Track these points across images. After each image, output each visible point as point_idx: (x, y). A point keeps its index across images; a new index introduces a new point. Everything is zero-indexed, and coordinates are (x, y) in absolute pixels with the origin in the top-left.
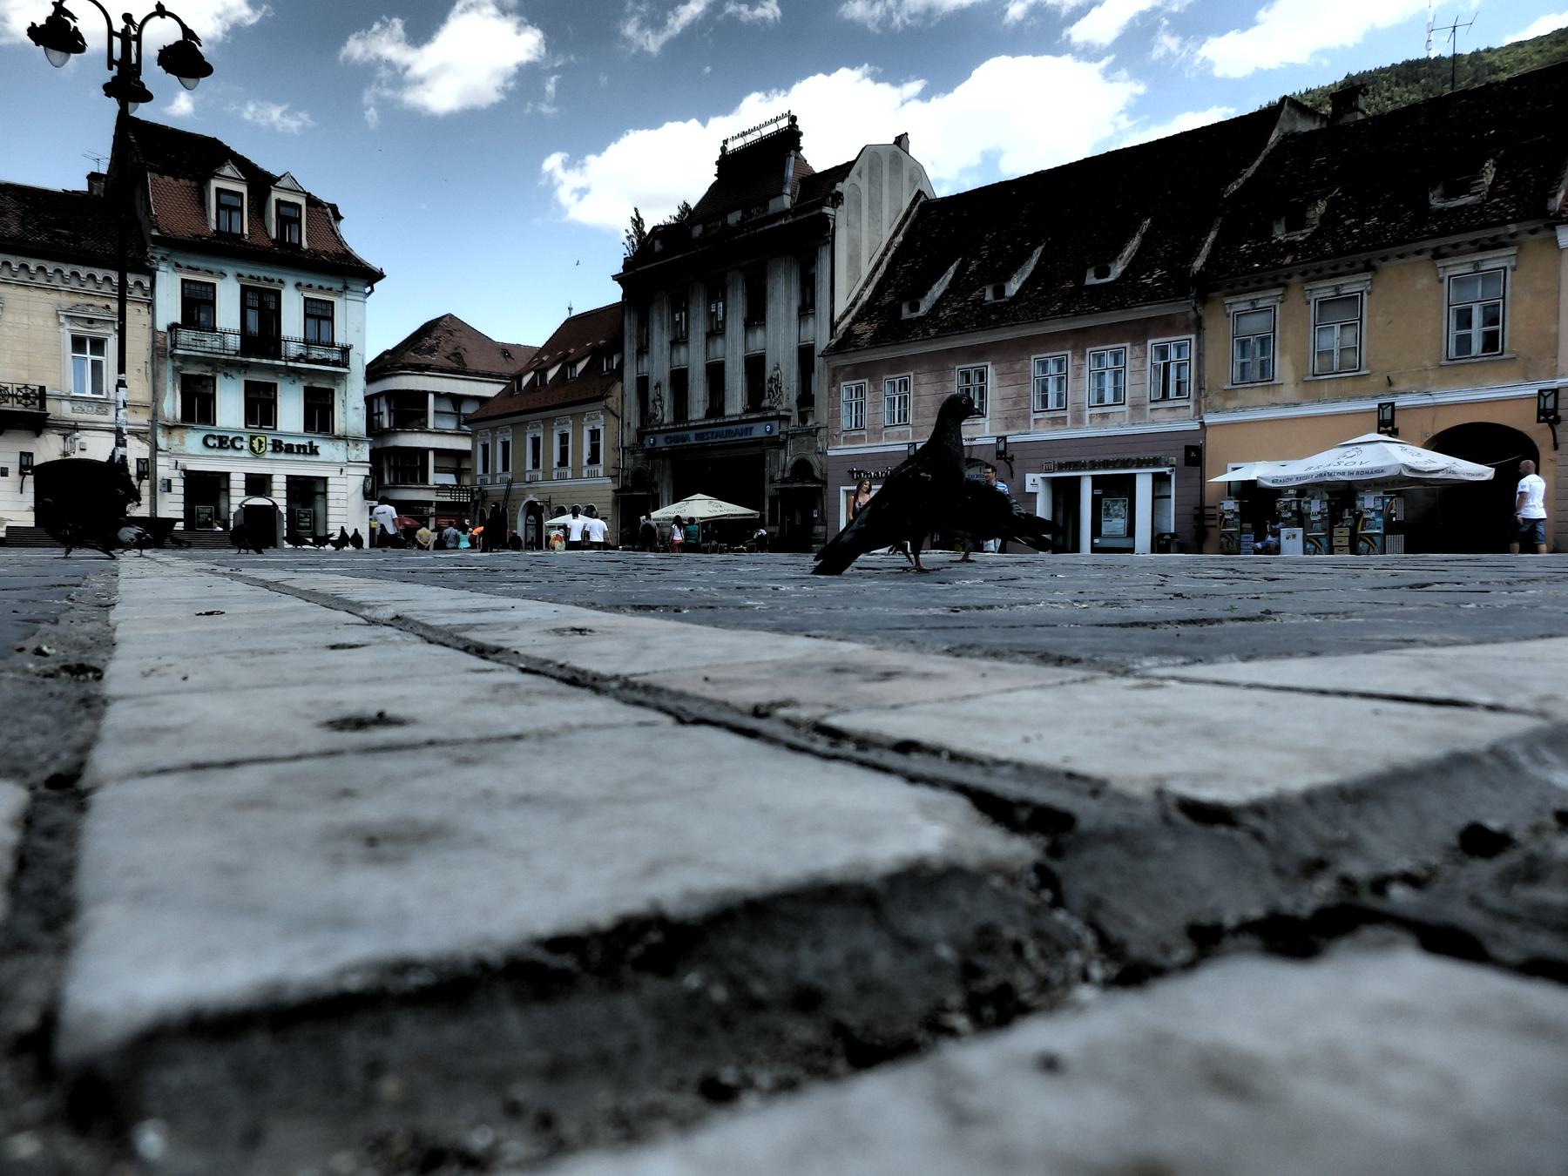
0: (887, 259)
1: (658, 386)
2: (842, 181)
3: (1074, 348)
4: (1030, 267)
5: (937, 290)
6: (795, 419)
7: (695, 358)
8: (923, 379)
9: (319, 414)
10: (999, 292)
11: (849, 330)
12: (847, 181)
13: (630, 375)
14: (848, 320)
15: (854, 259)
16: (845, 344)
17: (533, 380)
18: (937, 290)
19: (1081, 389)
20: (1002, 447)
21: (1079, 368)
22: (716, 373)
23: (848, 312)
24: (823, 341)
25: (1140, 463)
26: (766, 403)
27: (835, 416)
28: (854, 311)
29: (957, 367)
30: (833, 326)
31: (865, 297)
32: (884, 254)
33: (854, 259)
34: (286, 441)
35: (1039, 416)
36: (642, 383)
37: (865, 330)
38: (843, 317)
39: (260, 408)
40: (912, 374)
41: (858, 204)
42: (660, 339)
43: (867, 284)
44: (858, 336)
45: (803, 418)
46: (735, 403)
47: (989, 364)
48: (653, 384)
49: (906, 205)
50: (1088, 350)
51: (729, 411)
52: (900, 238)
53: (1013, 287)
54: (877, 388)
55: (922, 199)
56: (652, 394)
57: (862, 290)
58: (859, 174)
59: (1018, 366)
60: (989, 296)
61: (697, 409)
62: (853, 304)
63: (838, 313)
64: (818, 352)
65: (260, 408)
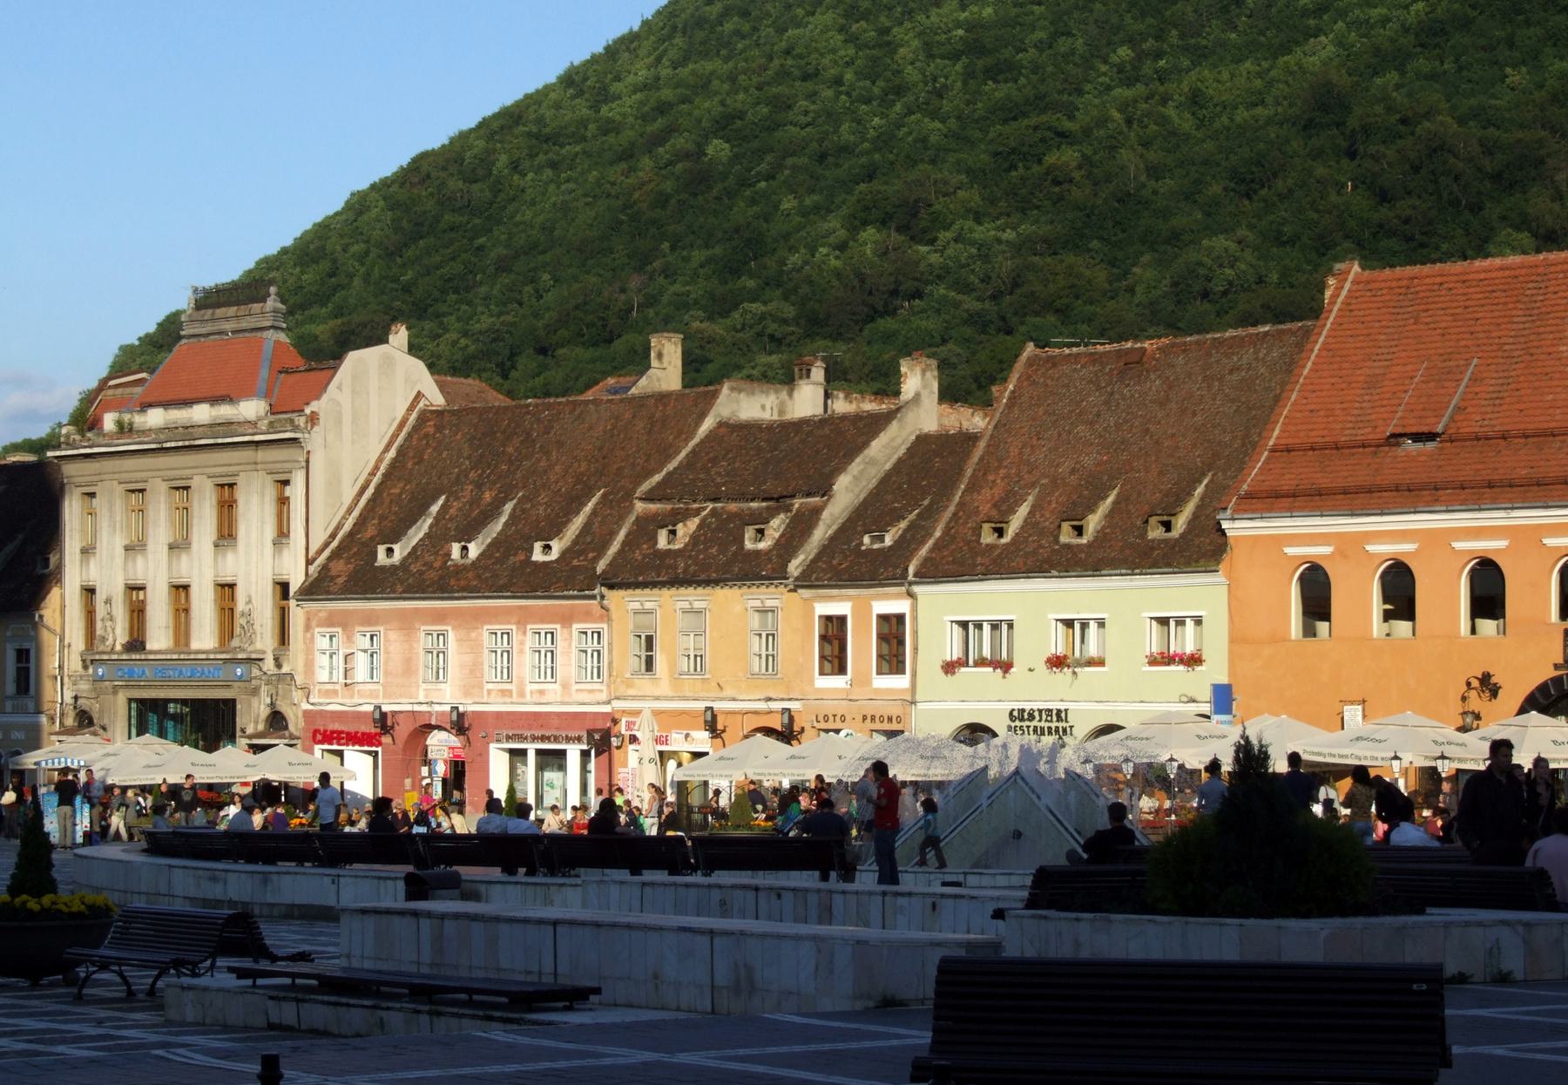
1: (108, 601)
2: (318, 397)
3: (518, 623)
6: (269, 665)
7: (155, 572)
8: (393, 635)
11: (325, 568)
12: (325, 398)
14: (327, 553)
15: (334, 482)
16: (315, 589)
19: (525, 663)
20: (454, 717)
21: (522, 643)
22: (181, 590)
23: (326, 545)
24: (296, 581)
25: (568, 740)
26: (235, 643)
27: (309, 666)
28: (335, 544)
29: (423, 628)
30: (309, 562)
32: (373, 474)
33: (334, 482)
35: (490, 686)
36: (90, 591)
37: (339, 567)
40: (381, 629)
41: (339, 421)
42: (112, 542)
43: (350, 511)
44: (333, 578)
45: (279, 666)
46: (204, 637)
47: (449, 628)
48: (100, 597)
49: (400, 413)
50: (529, 627)
51: (195, 645)
52: (392, 453)
54: (350, 639)
56: (101, 611)
57: (344, 518)
58: (339, 388)
59: (473, 635)
61: (159, 638)
62: (333, 536)
63: (314, 547)
64: (293, 589)
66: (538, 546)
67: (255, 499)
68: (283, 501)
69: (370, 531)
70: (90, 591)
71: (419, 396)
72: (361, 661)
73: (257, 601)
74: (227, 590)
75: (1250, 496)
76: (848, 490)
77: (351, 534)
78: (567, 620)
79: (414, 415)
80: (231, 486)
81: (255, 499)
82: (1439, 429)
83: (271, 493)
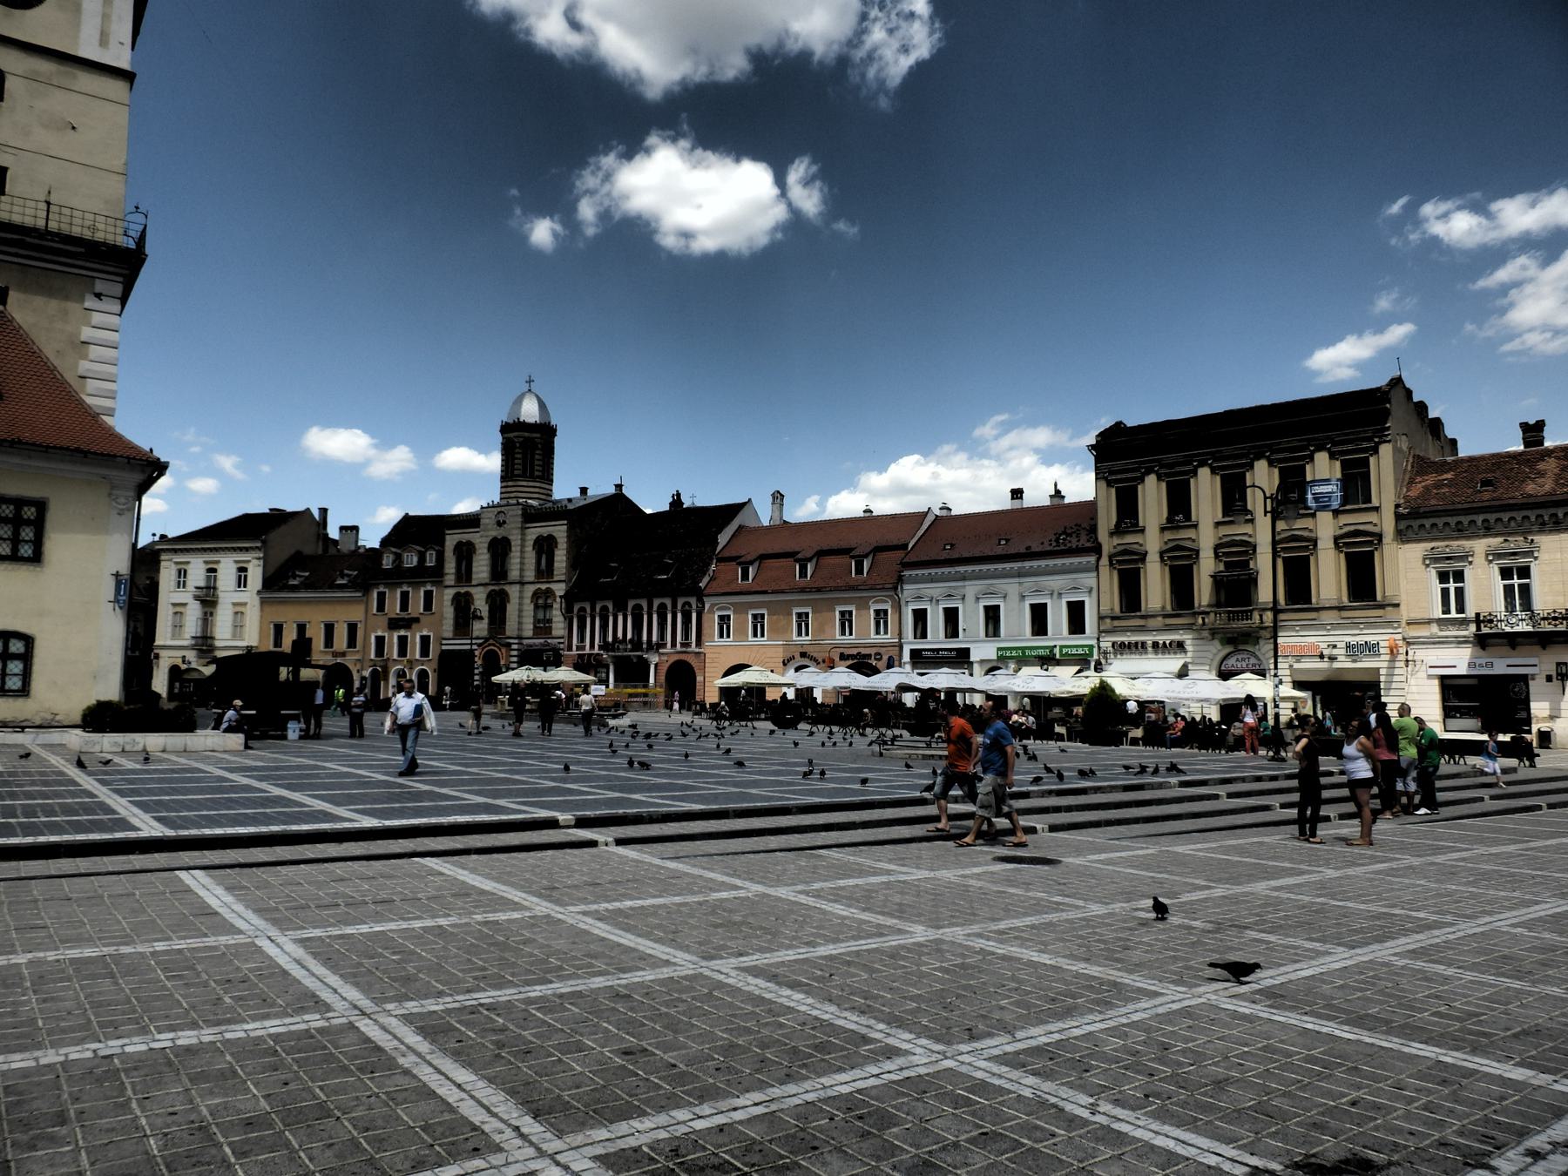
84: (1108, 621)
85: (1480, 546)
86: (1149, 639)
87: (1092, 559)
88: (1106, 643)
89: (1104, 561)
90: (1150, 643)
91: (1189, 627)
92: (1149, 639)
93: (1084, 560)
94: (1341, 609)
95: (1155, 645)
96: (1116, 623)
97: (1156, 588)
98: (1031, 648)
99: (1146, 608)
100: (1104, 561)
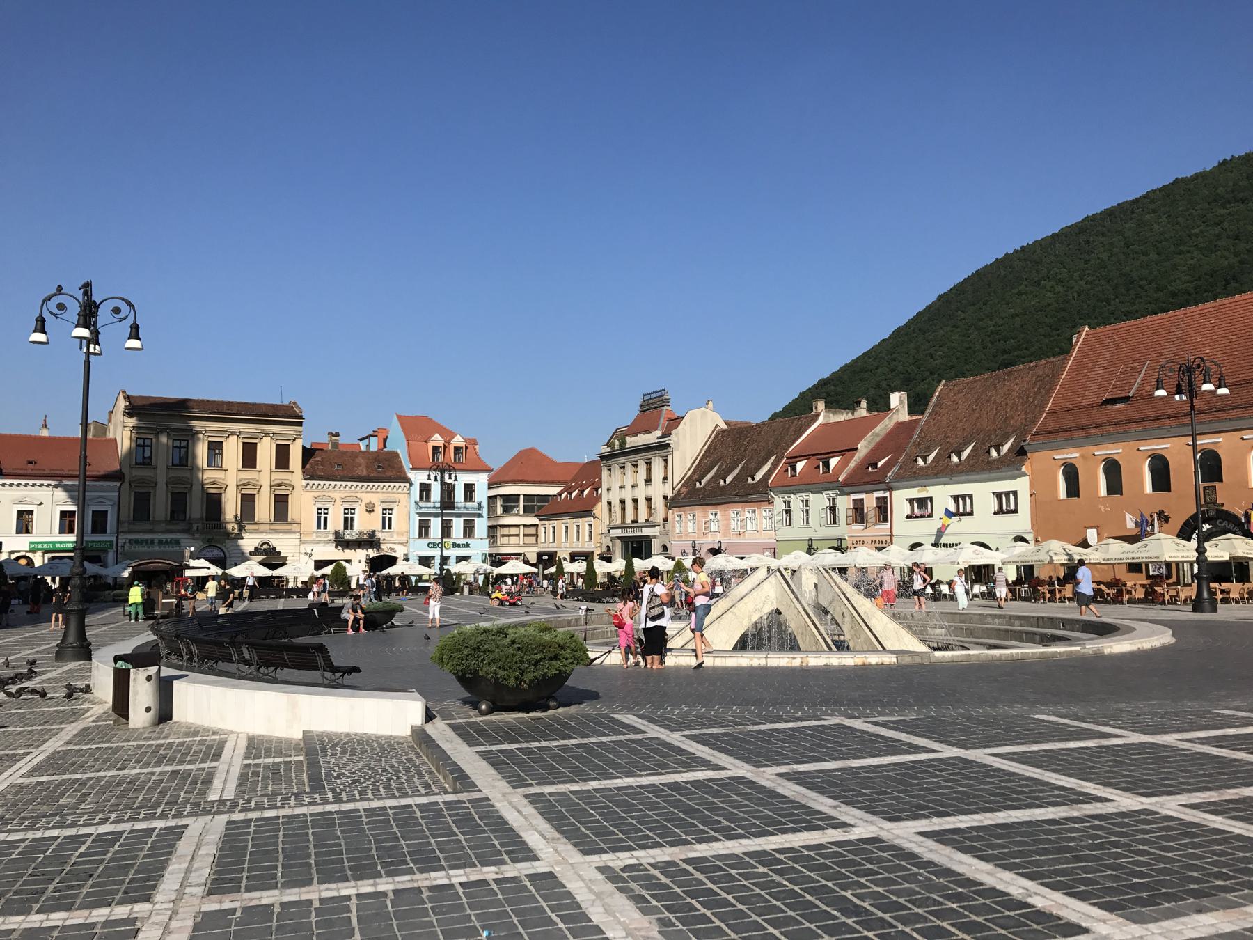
0: (699, 457)
1: (614, 507)
4: (736, 472)
5: (709, 476)
6: (662, 526)
8: (700, 514)
9: (469, 528)
10: (725, 482)
11: (679, 490)
13: (605, 500)
17: (566, 497)
18: (709, 476)
27: (674, 527)
30: (673, 489)
31: (688, 475)
32: (698, 455)
34: (457, 542)
36: (609, 503)
38: (677, 485)
39: (446, 529)
43: (689, 470)
52: (706, 447)
53: (729, 480)
55: (718, 428)
58: (685, 424)
60: (722, 482)
62: (683, 479)
65: (446, 529)
66: (750, 479)
67: (657, 467)
68: (666, 467)
69: (696, 476)
70: (609, 503)
71: (717, 425)
72: (690, 525)
73: (659, 504)
74: (649, 499)
75: (1037, 434)
76: (863, 448)
77: (689, 478)
78: (759, 507)
79: (715, 433)
80: (650, 463)
81: (657, 467)
82: (1130, 395)
83: (662, 464)
84: (126, 525)
85: (337, 496)
86: (156, 537)
87: (118, 484)
88: (124, 538)
89: (126, 485)
90: (156, 541)
91: (187, 531)
92: (156, 537)
93: (111, 484)
94: (271, 524)
95: (160, 542)
96: (132, 527)
97: (160, 505)
98: (61, 543)
99: (154, 517)
100: (126, 485)
